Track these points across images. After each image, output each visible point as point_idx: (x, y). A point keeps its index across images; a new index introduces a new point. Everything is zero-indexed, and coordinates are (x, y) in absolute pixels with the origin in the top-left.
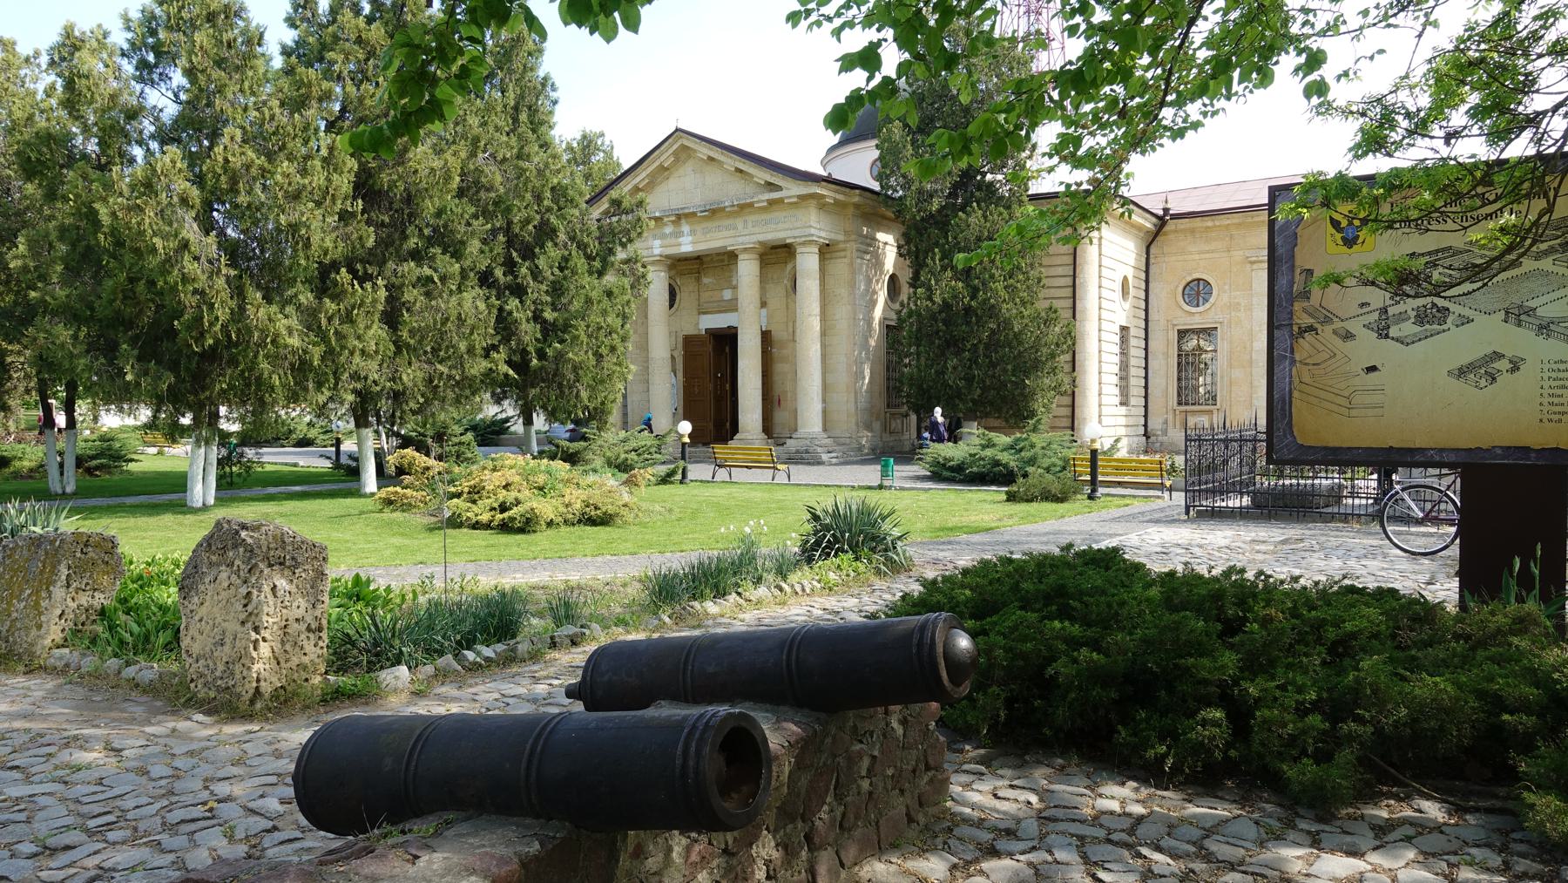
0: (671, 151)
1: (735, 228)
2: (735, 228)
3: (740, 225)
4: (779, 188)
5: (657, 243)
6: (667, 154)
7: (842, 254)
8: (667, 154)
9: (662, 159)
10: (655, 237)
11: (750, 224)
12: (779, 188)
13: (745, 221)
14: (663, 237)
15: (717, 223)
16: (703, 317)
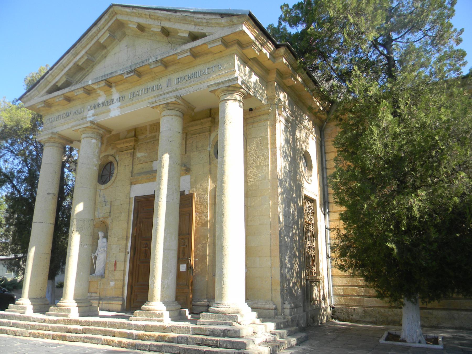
0: (107, 27)
1: (159, 88)
2: (159, 88)
3: (164, 82)
4: (204, 35)
5: (91, 112)
6: (103, 31)
7: (265, 117)
8: (103, 31)
9: (99, 35)
10: (90, 108)
11: (174, 82)
12: (204, 35)
13: (170, 80)
14: (97, 106)
15: (142, 87)
16: (135, 187)
